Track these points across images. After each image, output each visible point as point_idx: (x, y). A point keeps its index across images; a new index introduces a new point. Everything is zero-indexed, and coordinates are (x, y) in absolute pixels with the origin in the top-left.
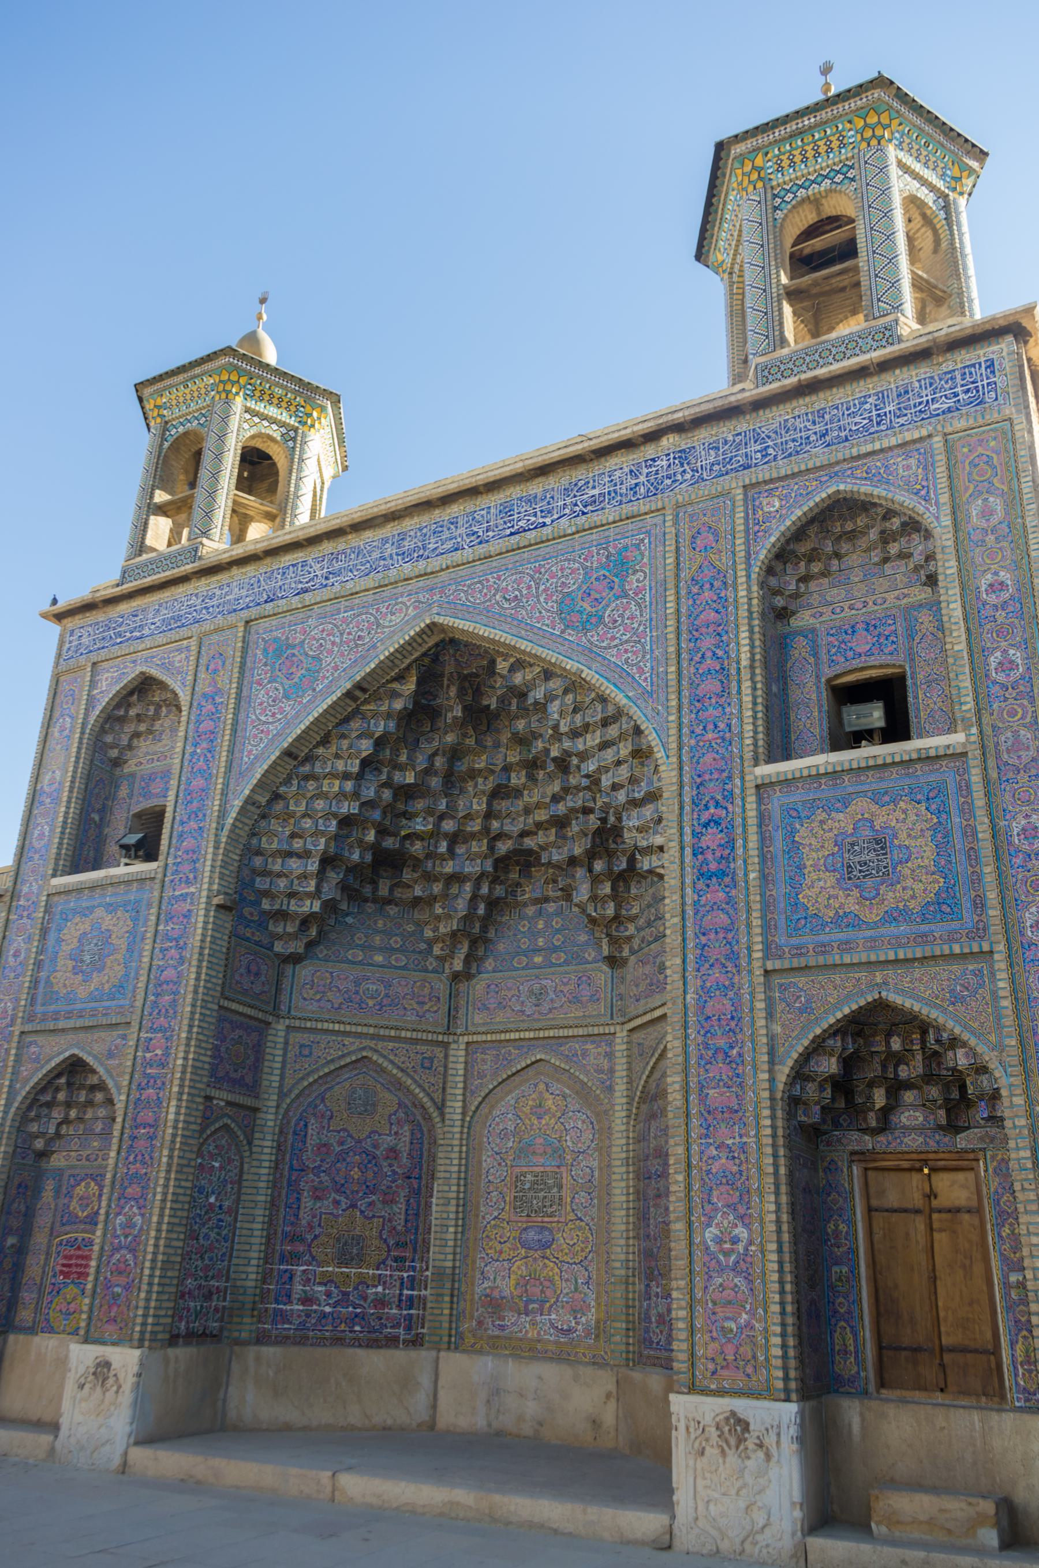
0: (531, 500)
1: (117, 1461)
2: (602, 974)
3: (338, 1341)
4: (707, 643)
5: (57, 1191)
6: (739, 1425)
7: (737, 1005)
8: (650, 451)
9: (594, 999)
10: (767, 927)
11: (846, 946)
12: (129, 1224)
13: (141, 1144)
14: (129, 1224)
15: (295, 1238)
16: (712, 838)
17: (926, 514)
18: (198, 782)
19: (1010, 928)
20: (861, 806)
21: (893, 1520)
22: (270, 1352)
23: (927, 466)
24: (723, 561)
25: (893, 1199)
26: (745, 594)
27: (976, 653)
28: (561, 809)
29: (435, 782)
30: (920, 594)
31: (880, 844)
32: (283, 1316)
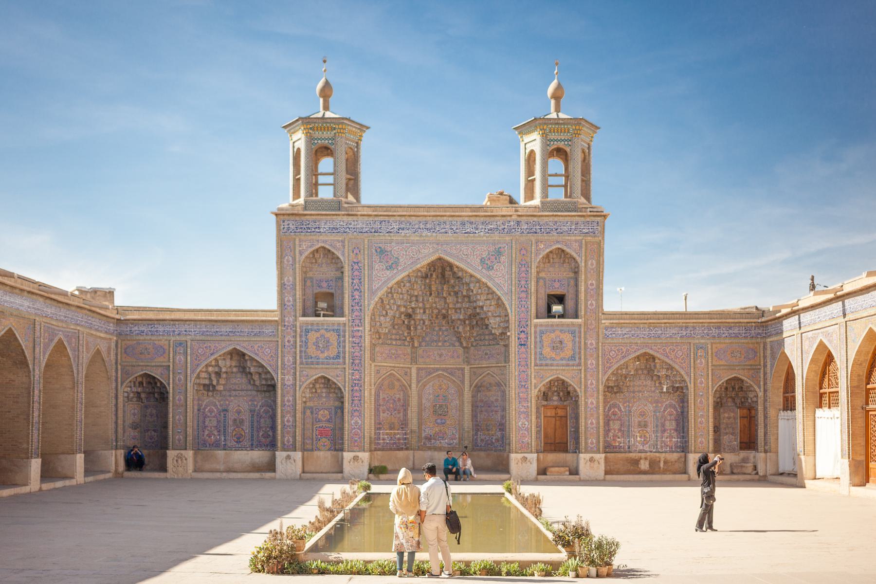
0: (471, 223)
1: (366, 477)
2: (461, 351)
3: (391, 449)
4: (523, 283)
5: (312, 413)
6: (525, 459)
7: (527, 375)
8: (509, 218)
9: (458, 357)
10: (535, 359)
11: (552, 365)
12: (356, 423)
13: (356, 402)
14: (356, 423)
15: (380, 424)
16: (522, 335)
17: (579, 261)
18: (356, 293)
19: (586, 364)
20: (558, 332)
21: (551, 472)
22: (379, 452)
23: (581, 247)
24: (528, 260)
25: (549, 414)
26: (534, 270)
27: (586, 300)
28: (459, 305)
29: (420, 293)
30: (572, 275)
31: (561, 342)
32: (379, 444)
